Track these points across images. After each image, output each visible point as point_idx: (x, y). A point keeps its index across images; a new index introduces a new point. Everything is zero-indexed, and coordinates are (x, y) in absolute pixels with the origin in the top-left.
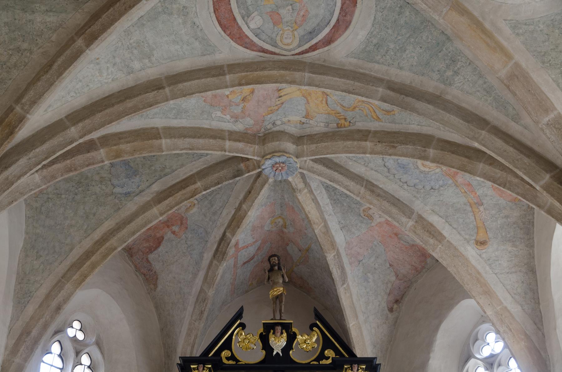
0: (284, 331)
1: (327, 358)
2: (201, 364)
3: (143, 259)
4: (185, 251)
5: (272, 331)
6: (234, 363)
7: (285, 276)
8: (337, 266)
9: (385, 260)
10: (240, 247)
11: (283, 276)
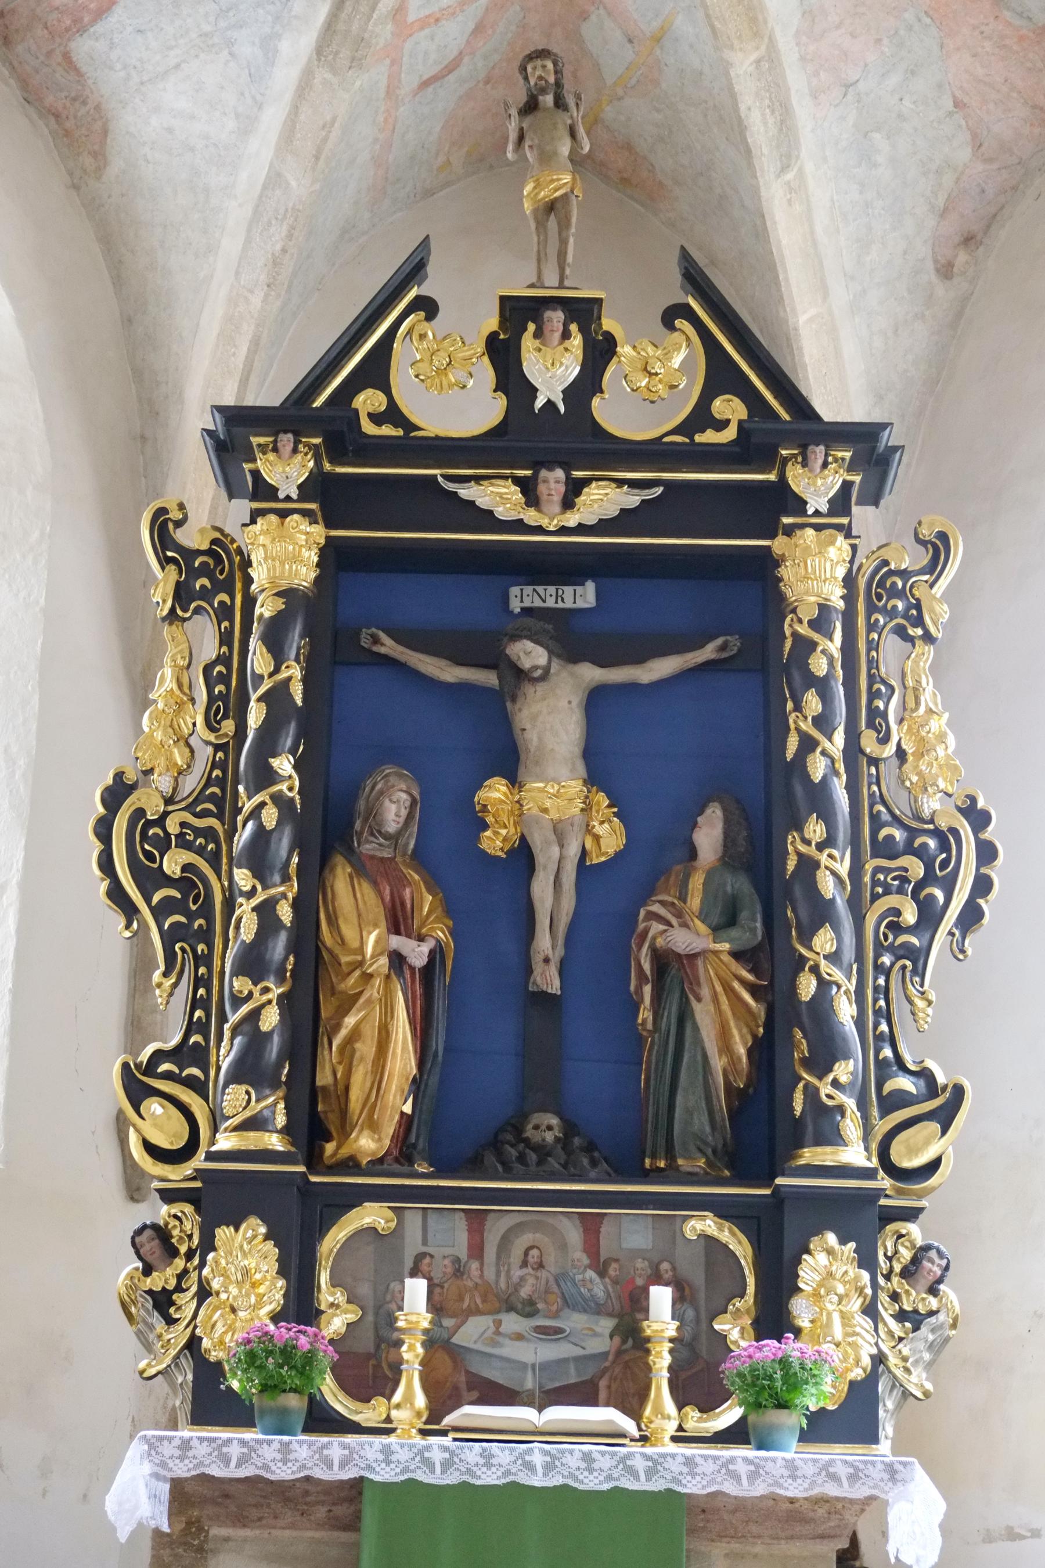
0: (574, 327)
1: (721, 425)
2: (286, 432)
3: (49, 54)
4: (207, 28)
5: (531, 327)
6: (400, 432)
7: (581, 131)
8: (767, 102)
9: (940, 86)
10: (411, 17)
11: (573, 134)
